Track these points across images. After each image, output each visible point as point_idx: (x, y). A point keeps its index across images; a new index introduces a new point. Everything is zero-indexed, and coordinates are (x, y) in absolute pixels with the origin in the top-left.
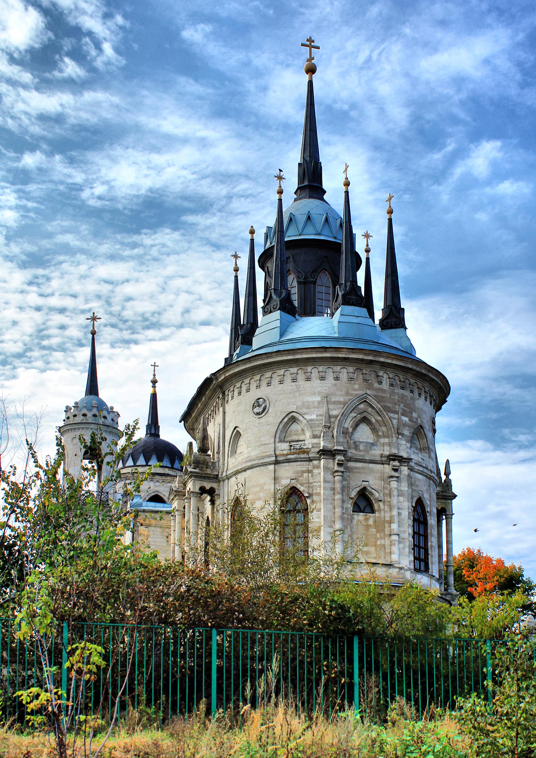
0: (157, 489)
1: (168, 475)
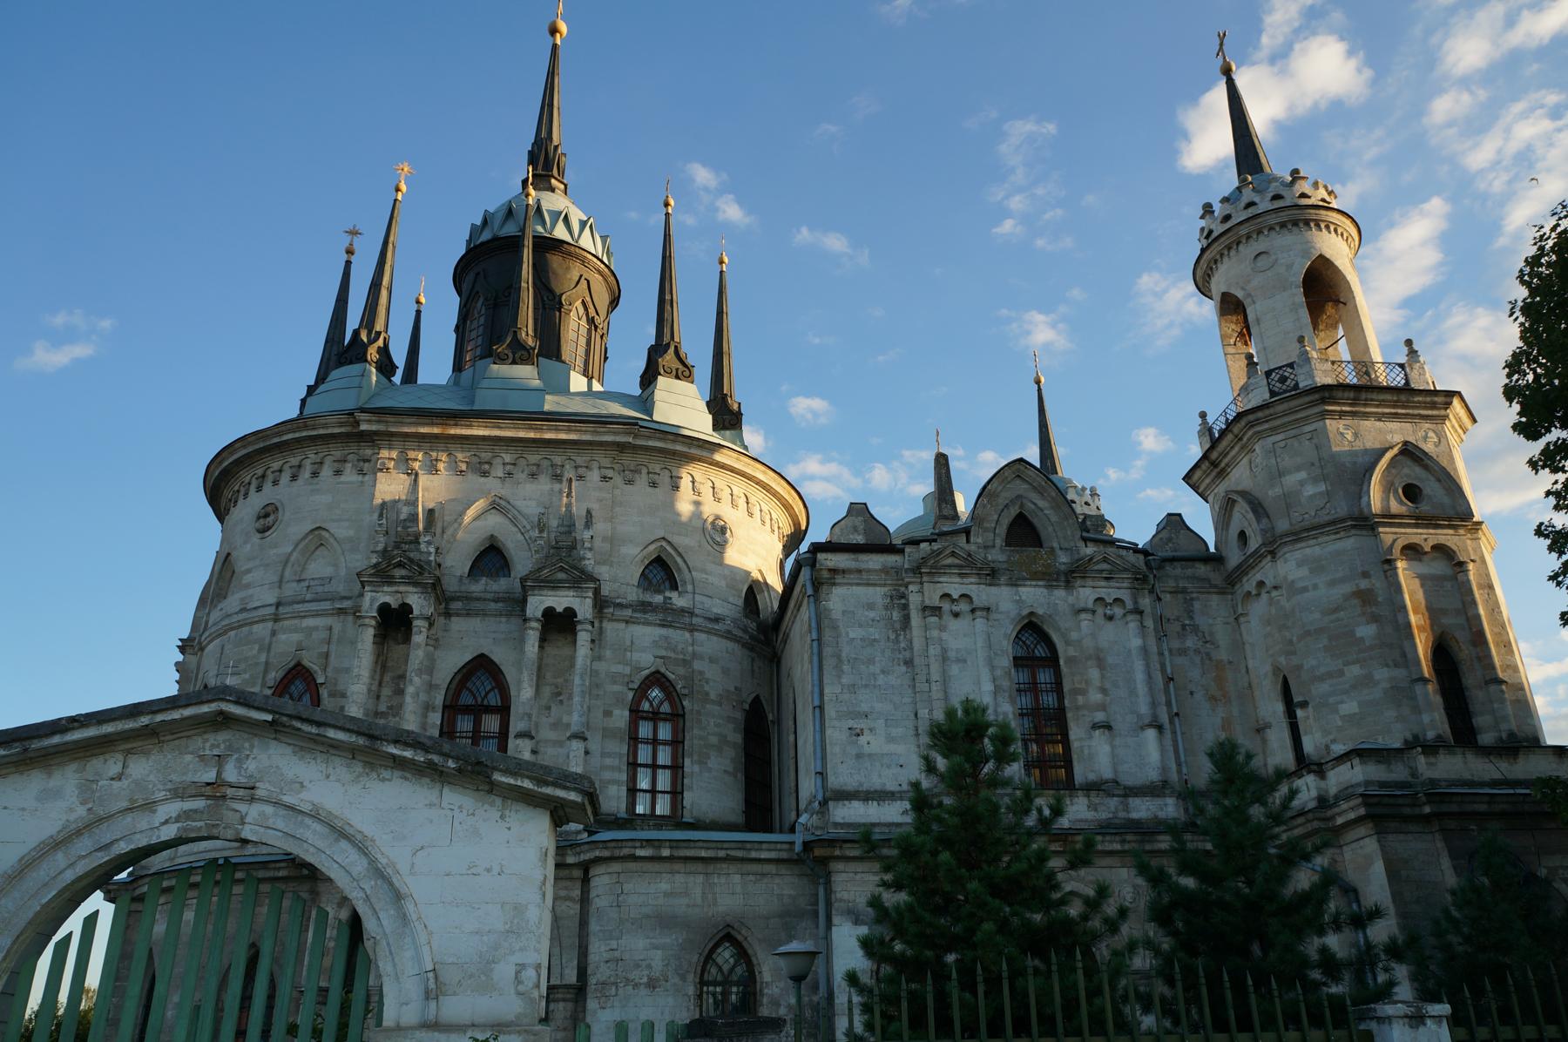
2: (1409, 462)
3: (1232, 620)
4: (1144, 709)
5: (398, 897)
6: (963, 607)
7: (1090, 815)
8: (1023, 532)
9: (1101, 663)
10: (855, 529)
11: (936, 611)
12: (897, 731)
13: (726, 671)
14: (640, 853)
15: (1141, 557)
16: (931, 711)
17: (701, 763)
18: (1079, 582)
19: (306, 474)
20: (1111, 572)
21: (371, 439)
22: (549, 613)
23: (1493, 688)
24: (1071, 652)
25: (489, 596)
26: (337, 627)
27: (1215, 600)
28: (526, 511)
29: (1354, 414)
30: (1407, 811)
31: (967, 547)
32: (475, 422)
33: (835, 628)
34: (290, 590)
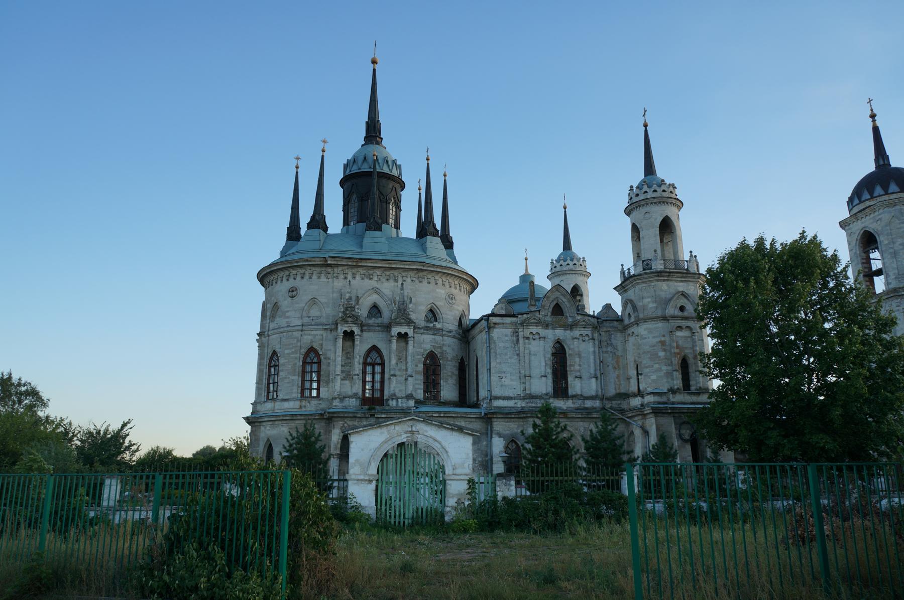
0: (863, 225)
1: (870, 206)
2: (683, 298)
3: (623, 341)
4: (592, 371)
5: (447, 452)
6: (537, 336)
7: (572, 406)
9: (580, 356)
10: (502, 308)
11: (528, 338)
12: (515, 377)
13: (453, 349)
14: (434, 415)
15: (596, 319)
17: (446, 382)
18: (575, 329)
19: (307, 277)
20: (585, 325)
21: (331, 266)
22: (399, 334)
24: (571, 352)
25: (376, 325)
26: (324, 333)
27: (619, 334)
28: (386, 293)
29: (668, 280)
30: (664, 411)
31: (538, 316)
32: (368, 261)
33: (495, 343)
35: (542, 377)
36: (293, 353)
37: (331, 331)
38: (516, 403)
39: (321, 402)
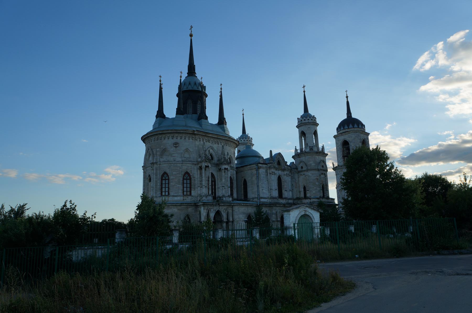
1: (347, 131)
4: (290, 188)
5: (314, 218)
6: (273, 173)
7: (285, 202)
8: (279, 163)
11: (270, 174)
14: (242, 204)
16: (270, 187)
21: (195, 134)
23: (327, 191)
28: (215, 149)
34: (183, 159)
35: (275, 190)
36: (178, 174)
37: (195, 165)
38: (267, 200)
39: (192, 197)
